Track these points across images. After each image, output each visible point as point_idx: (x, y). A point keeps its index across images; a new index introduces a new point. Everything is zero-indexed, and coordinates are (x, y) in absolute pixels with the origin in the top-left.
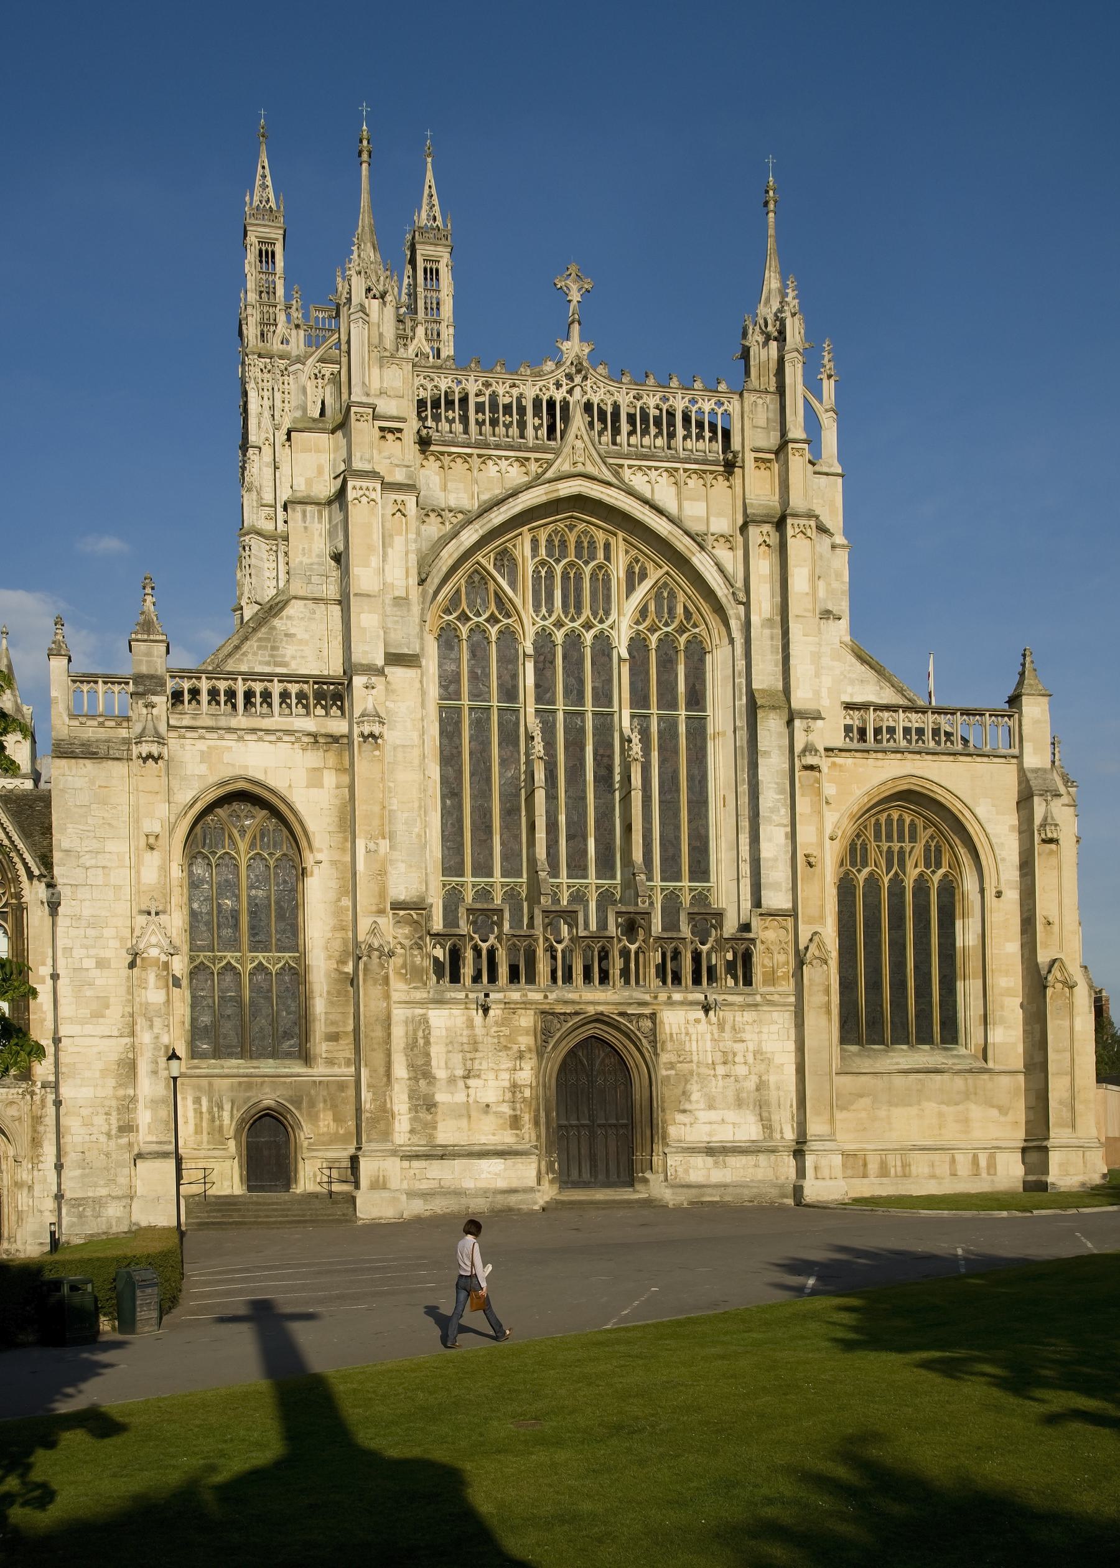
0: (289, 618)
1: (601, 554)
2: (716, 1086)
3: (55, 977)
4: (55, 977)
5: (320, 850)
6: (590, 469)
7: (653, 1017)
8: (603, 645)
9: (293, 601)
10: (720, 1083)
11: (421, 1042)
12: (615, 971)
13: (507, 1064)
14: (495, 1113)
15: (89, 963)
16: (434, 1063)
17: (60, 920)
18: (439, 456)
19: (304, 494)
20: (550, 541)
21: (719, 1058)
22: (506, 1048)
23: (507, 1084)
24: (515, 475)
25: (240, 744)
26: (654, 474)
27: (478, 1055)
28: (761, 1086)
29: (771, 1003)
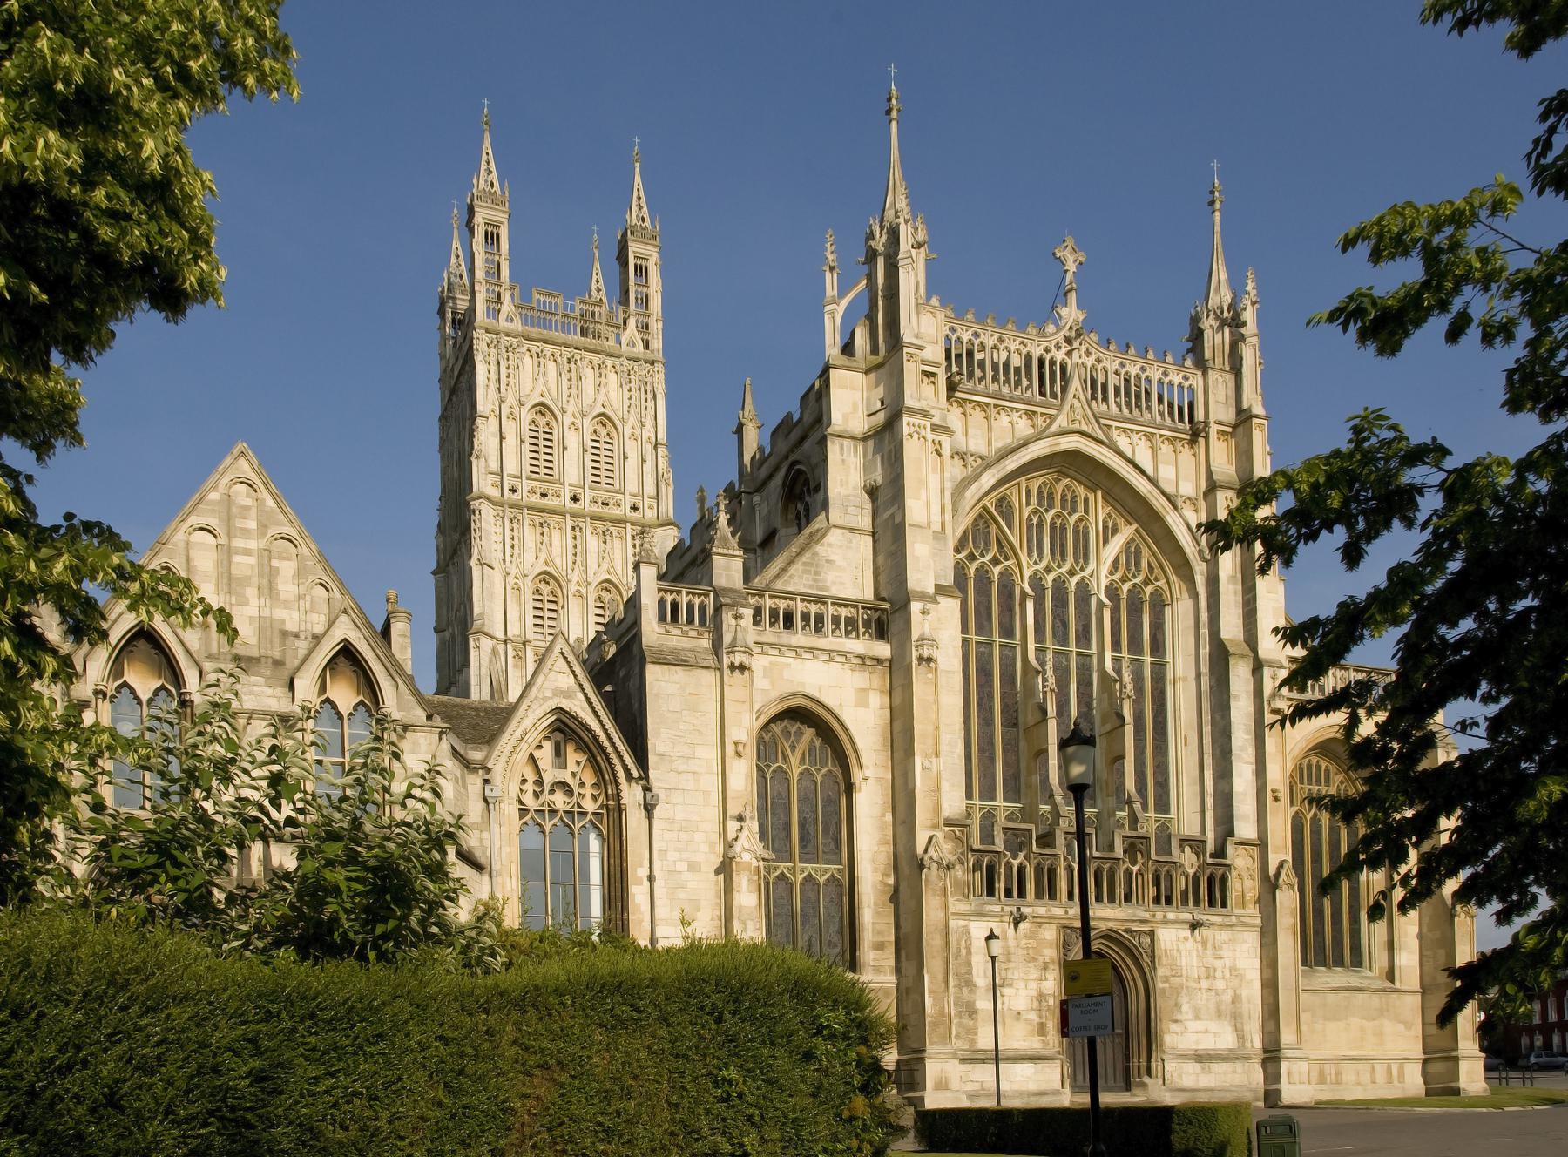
0: (830, 545)
1: (1081, 507)
2: (1202, 999)
3: (651, 878)
4: (651, 878)
5: (868, 768)
6: (1084, 427)
7: (1152, 934)
8: (1084, 591)
9: (833, 530)
10: (1204, 996)
11: (964, 951)
12: (1120, 891)
13: (1034, 974)
14: (1026, 1020)
15: (681, 866)
16: (975, 971)
17: (656, 822)
18: (962, 403)
19: (841, 428)
20: (1040, 492)
21: (1203, 973)
22: (1034, 959)
23: (1034, 993)
24: (1024, 427)
25: (798, 661)
26: (1135, 437)
27: (1011, 965)
28: (1236, 1000)
29: (1245, 925)
